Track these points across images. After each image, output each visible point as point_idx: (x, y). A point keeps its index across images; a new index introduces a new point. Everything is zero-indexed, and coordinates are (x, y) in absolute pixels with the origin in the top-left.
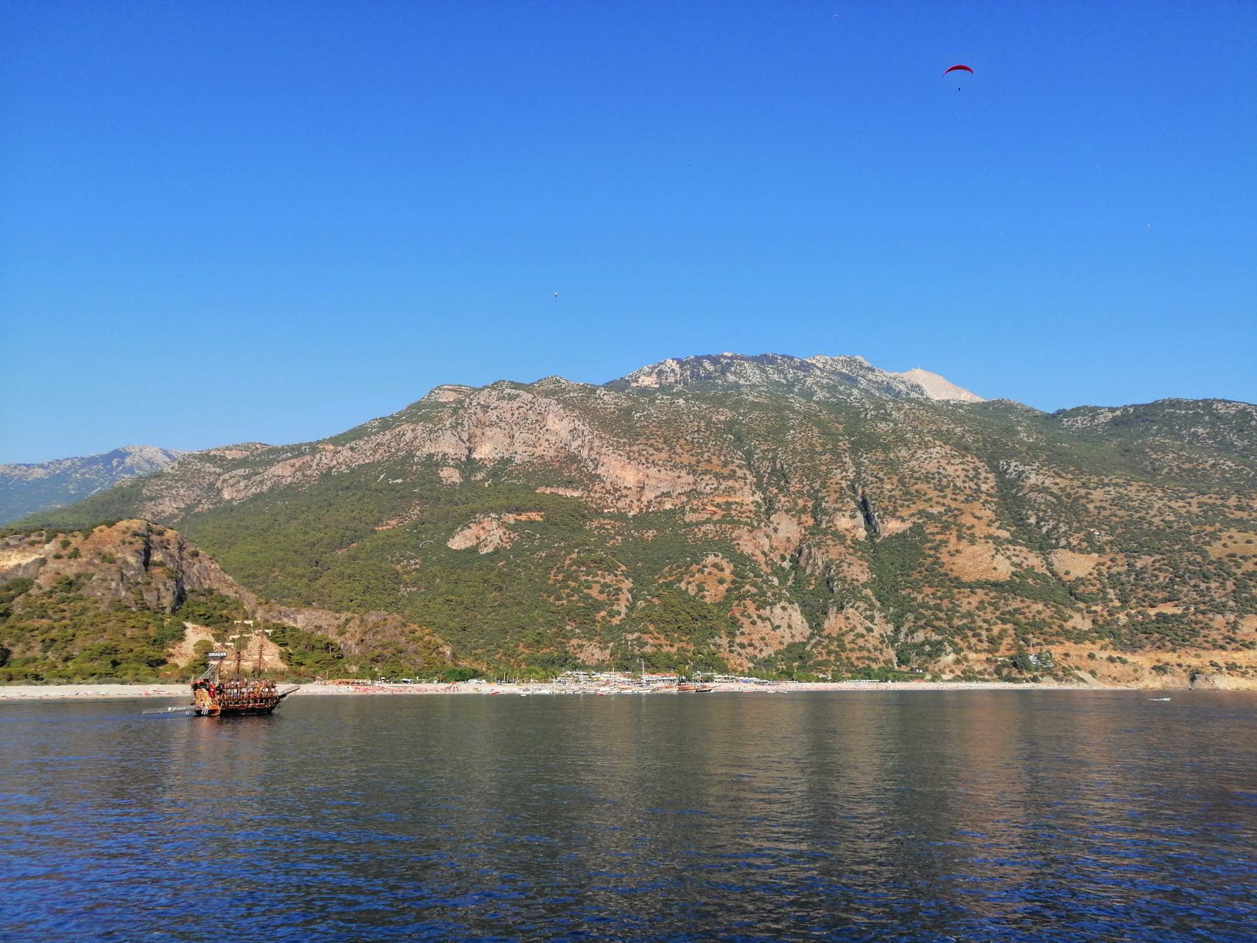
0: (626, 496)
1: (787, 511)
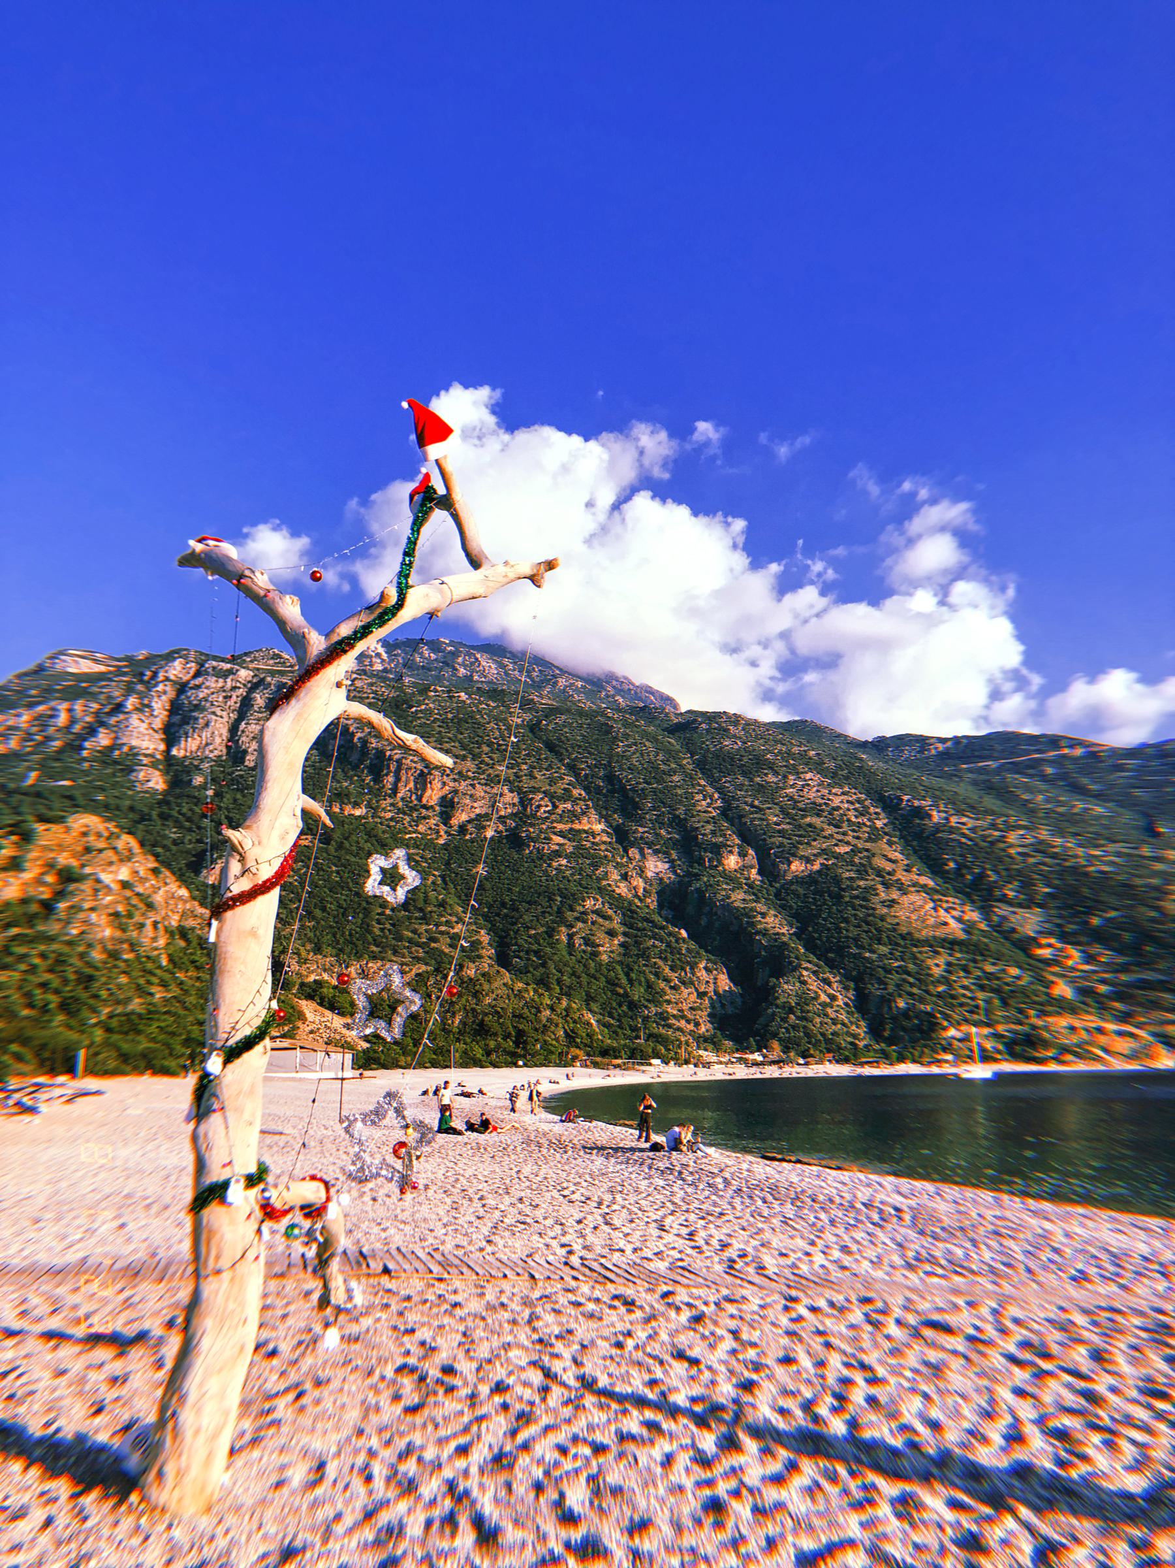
1: (650, 845)
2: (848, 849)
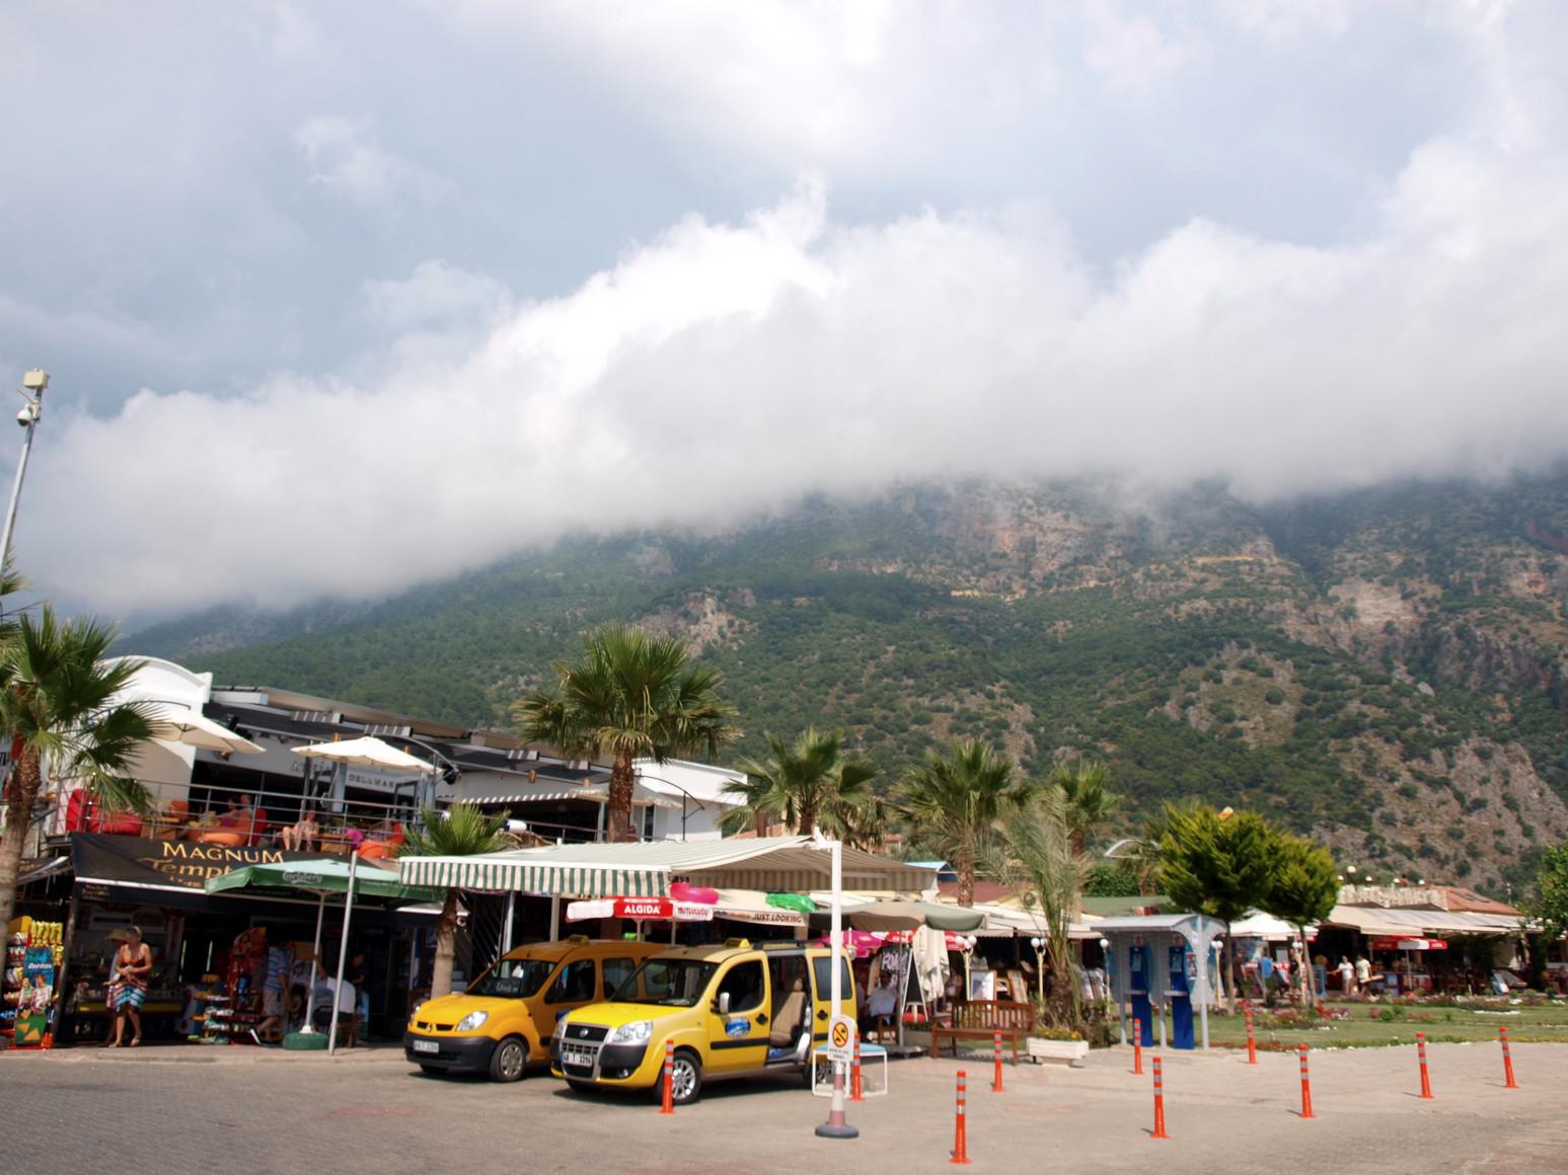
0: (997, 569)
1: (1368, 576)
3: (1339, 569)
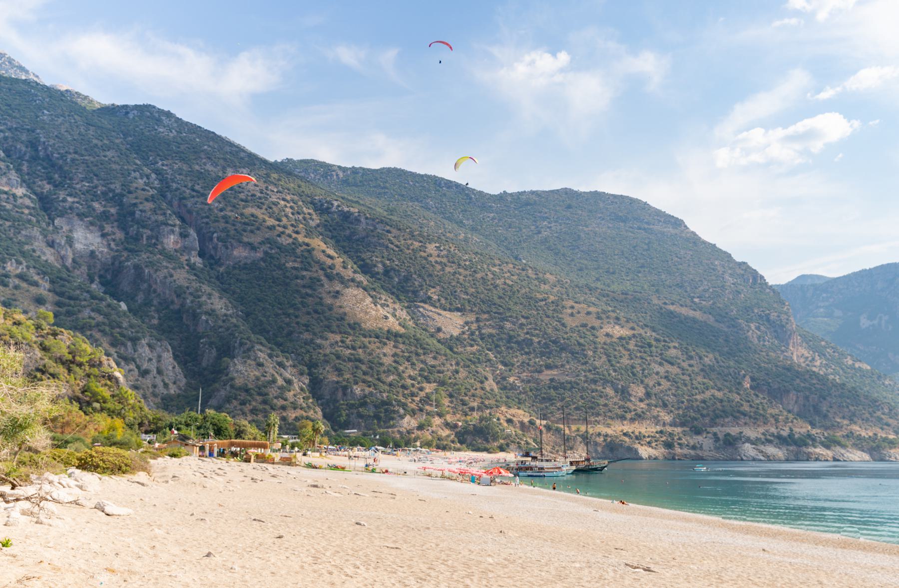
1: (81, 216)
2: (290, 241)
3: (63, 206)
